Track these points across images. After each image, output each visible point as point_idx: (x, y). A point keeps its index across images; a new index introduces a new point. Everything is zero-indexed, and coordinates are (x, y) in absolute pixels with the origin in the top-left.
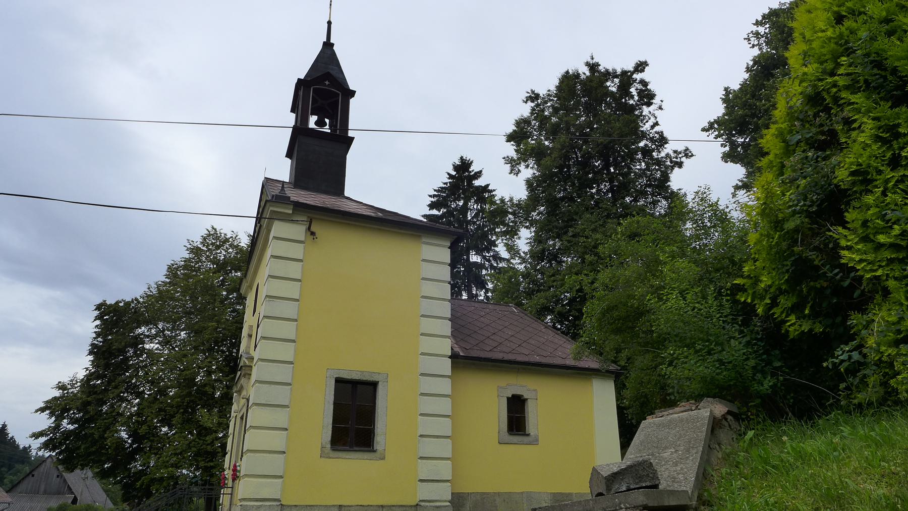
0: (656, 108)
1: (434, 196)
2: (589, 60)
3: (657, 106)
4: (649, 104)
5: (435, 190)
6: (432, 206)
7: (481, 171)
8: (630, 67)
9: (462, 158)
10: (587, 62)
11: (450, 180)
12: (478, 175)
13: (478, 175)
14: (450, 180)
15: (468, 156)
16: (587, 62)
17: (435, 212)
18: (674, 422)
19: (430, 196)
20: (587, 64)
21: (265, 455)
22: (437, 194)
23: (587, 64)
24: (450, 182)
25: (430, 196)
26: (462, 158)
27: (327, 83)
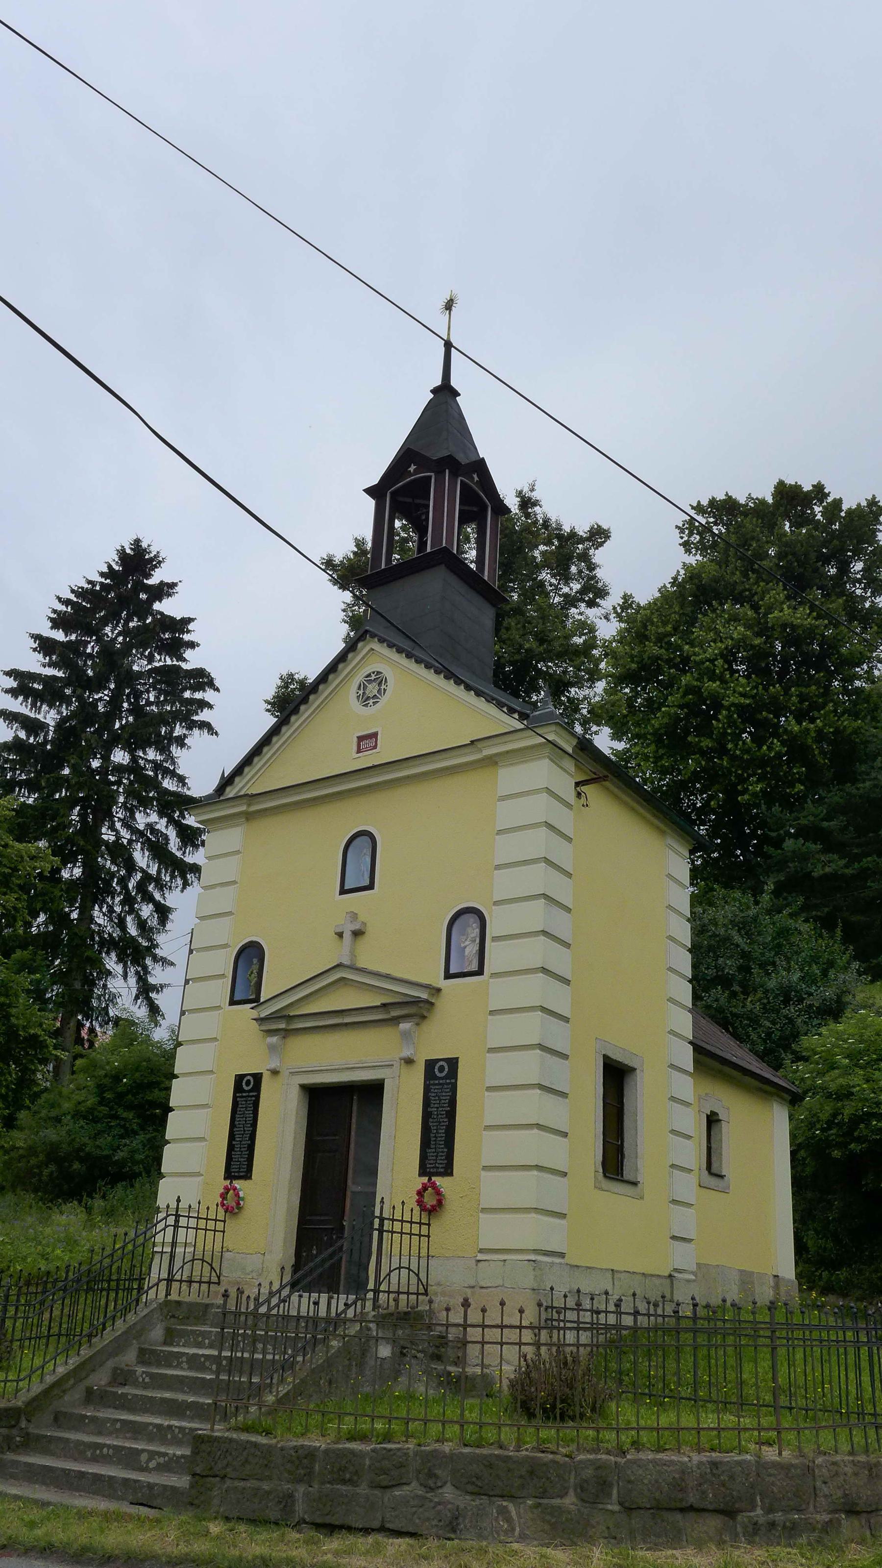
0: (599, 614)
1: (67, 602)
2: (526, 490)
3: (603, 611)
4: (591, 604)
5: (73, 591)
6: (58, 622)
7: (173, 585)
8: (582, 530)
9: (137, 542)
10: (521, 492)
11: (103, 580)
12: (164, 590)
13: (164, 590)
14: (103, 580)
15: (154, 544)
16: (521, 492)
17: (59, 636)
18: (420, 1355)
19: (59, 599)
20: (520, 494)
21: (189, 1145)
22: (75, 599)
23: (520, 494)
24: (102, 584)
25: (59, 599)
26: (137, 542)
27: (476, 478)
